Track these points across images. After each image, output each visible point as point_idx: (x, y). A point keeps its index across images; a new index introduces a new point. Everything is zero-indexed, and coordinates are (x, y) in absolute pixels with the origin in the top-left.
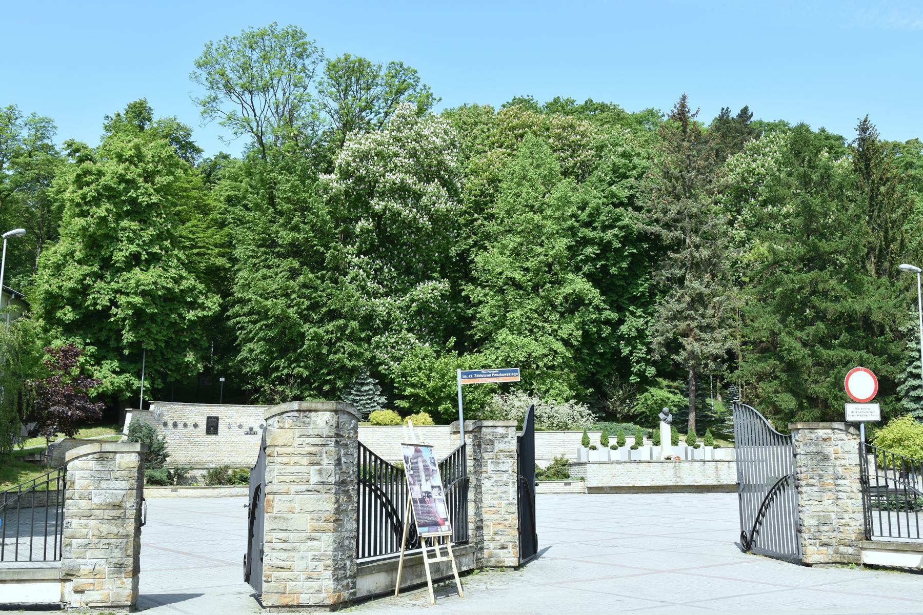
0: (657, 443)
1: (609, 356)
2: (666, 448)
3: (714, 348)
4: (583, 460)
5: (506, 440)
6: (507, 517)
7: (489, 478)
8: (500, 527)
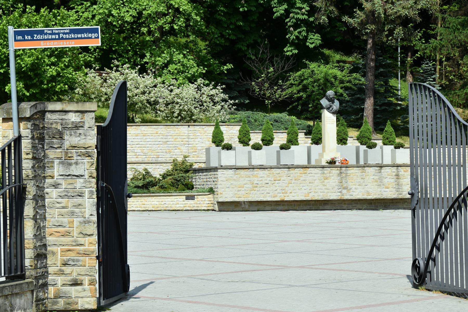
0: (317, 141)
1: (255, 17)
2: (330, 147)
4: (214, 164)
5: (80, 131)
6: (81, 240)
7: (56, 186)
8: (72, 255)
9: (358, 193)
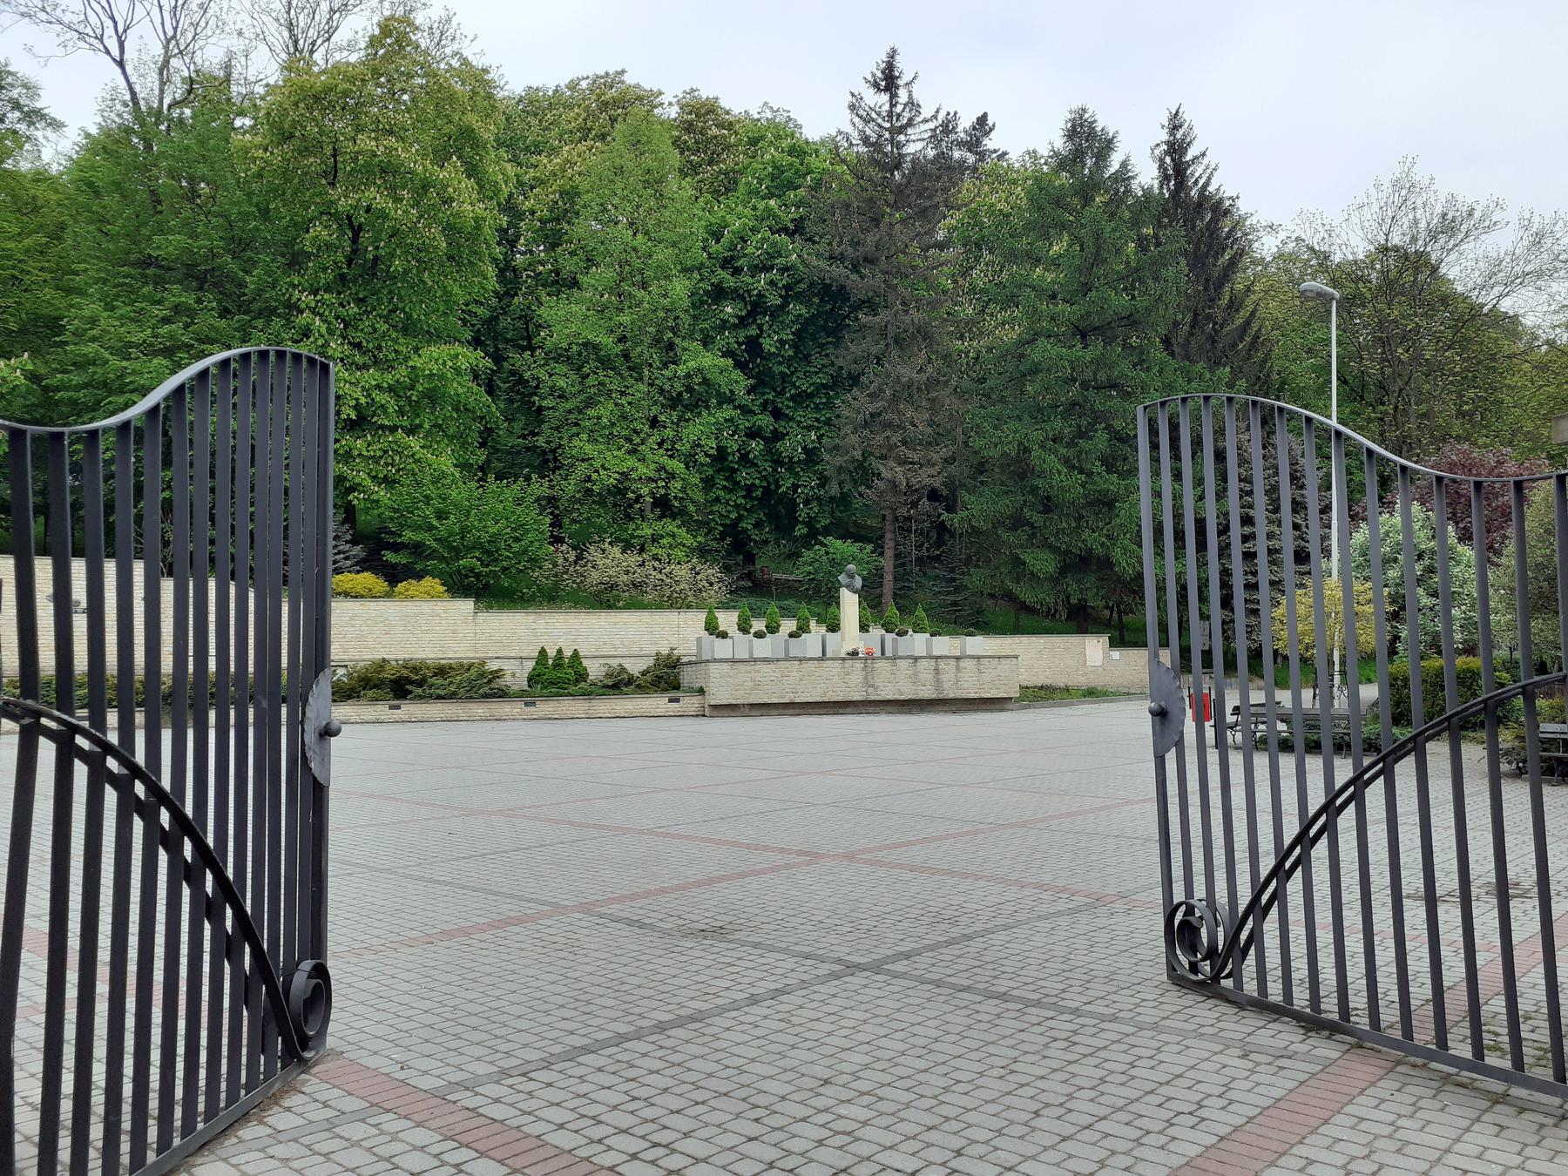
0: (834, 628)
1: (759, 493)
2: (850, 635)
3: (928, 477)
9: (887, 693)
